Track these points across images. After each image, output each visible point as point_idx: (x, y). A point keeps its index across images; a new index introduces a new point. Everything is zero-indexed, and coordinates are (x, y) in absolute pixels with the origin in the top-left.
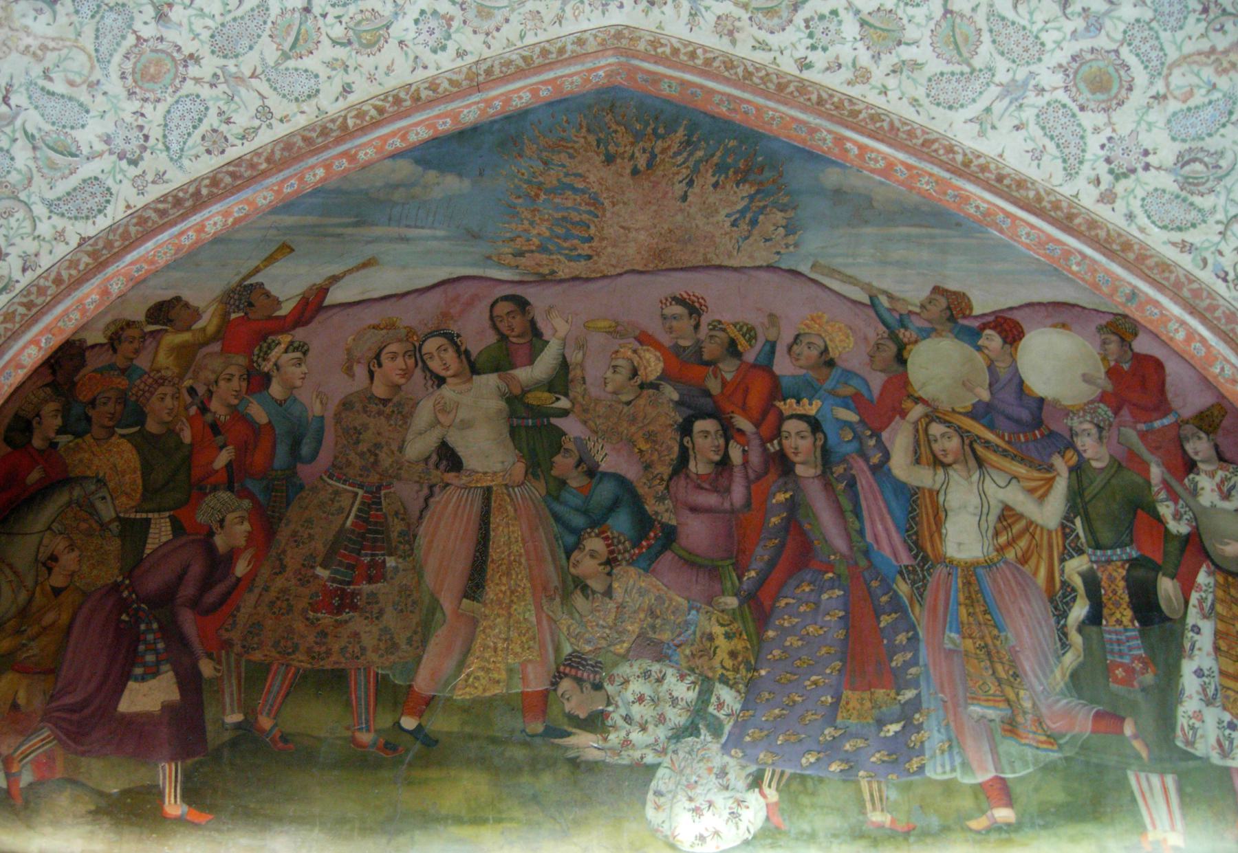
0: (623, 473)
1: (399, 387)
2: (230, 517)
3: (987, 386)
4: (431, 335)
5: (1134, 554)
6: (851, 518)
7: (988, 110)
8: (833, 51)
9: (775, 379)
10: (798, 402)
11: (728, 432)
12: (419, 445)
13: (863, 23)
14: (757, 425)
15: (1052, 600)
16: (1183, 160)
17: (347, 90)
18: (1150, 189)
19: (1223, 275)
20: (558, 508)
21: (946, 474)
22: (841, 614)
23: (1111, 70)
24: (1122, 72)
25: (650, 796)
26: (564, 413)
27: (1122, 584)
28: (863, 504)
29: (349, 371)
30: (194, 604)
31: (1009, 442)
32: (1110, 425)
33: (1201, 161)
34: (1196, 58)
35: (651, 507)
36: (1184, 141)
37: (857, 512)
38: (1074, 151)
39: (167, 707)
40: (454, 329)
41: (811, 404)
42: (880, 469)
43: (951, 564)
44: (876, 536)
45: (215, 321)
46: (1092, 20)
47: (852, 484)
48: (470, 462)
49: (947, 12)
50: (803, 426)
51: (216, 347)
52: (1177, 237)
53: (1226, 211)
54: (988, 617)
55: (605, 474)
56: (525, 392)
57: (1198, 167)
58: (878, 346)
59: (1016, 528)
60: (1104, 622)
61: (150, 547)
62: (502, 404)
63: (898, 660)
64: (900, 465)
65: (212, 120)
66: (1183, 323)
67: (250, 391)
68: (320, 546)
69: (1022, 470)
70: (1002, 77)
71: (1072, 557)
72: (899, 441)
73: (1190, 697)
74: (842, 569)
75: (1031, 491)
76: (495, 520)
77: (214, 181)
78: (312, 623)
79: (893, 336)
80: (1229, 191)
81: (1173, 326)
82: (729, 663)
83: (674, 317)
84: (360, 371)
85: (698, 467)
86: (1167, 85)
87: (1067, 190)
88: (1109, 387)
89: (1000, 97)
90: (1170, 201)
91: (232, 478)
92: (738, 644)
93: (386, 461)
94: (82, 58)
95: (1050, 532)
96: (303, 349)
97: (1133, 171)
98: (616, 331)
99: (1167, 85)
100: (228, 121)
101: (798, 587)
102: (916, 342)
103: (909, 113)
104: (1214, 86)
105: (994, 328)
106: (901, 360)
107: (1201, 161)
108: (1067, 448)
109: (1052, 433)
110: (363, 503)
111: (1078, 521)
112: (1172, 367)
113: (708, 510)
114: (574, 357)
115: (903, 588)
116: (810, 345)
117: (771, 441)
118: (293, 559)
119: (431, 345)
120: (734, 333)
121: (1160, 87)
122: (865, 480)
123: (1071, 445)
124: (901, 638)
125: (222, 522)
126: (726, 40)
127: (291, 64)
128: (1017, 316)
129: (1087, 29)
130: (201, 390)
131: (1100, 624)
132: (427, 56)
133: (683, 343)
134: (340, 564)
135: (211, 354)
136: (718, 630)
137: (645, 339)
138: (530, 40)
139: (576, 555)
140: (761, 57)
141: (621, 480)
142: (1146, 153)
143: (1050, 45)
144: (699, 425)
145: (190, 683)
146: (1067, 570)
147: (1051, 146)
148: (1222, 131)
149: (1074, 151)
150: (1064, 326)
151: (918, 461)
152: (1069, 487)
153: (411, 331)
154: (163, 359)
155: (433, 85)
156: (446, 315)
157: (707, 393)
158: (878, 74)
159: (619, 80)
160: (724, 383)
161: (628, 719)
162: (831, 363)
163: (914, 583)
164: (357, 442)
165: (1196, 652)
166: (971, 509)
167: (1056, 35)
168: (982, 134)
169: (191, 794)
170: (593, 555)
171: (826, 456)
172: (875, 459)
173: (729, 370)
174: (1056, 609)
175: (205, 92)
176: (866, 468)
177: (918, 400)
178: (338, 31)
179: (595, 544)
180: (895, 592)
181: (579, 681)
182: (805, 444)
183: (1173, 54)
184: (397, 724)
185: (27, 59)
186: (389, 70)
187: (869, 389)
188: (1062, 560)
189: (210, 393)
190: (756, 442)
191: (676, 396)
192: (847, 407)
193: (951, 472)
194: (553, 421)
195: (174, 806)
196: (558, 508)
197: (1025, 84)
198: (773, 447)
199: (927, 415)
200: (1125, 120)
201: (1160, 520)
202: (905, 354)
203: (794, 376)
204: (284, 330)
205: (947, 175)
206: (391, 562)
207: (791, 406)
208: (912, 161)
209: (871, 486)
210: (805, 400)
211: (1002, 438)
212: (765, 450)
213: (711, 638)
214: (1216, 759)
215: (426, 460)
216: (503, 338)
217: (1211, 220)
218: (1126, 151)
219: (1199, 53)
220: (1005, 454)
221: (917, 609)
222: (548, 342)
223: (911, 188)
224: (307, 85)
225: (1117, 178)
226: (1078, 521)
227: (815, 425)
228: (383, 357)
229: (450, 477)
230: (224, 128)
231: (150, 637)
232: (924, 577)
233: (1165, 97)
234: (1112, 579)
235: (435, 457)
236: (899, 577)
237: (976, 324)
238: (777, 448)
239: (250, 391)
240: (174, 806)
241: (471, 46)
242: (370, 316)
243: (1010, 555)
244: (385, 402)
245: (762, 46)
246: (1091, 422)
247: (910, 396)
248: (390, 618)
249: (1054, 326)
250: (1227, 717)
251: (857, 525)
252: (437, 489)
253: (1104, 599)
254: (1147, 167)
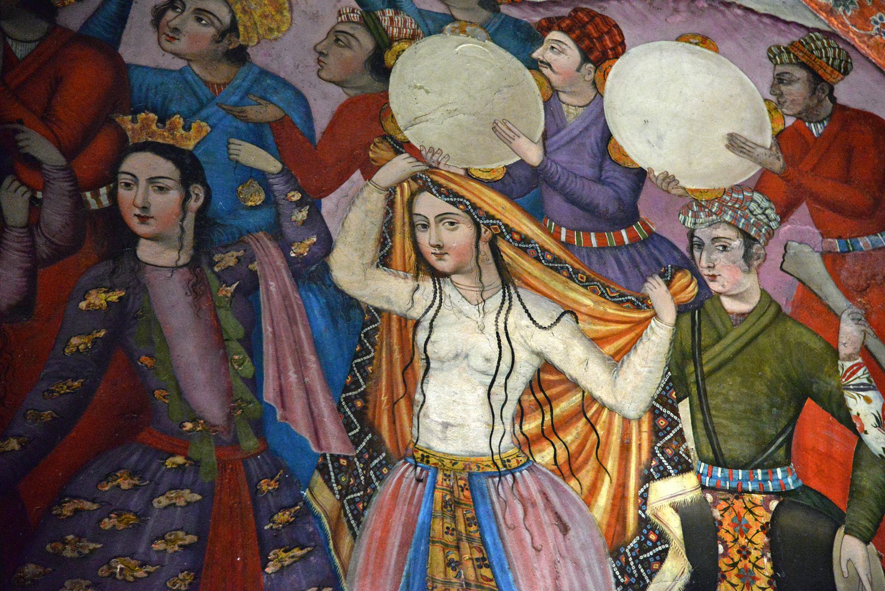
3: (538, 135)
5: (791, 483)
6: (238, 353)
9: (122, 69)
10: (162, 121)
14: (70, 152)
15: (615, 553)
21: (438, 291)
22: (190, 539)
27: (761, 539)
28: (267, 329)
31: (567, 245)
32: (771, 234)
41: (187, 128)
43: (424, 459)
50: (165, 167)
54: (486, 572)
58: (337, 37)
59: (563, 407)
69: (585, 300)
71: (664, 474)
72: (354, 216)
74: (207, 453)
75: (597, 341)
88: (778, 165)
95: (626, 420)
101: (106, 478)
102: (413, 38)
105: (567, 31)
106: (380, 69)
108: (678, 269)
109: (653, 238)
111: (684, 408)
115: (323, 498)
117: (94, 189)
122: (275, 285)
123: (689, 265)
151: (384, 261)
152: (673, 342)
163: (346, 490)
166: (477, 362)
171: (207, 232)
172: (300, 250)
174: (623, 570)
176: (280, 262)
177: (402, 146)
180: (306, 504)
192: (259, 142)
193: (448, 289)
199: (414, 178)
202: (389, 57)
207: (146, 125)
209: (285, 297)
210: (178, 120)
211: (556, 237)
212: (80, 203)
220: (555, 265)
221: (346, 540)
226: (684, 408)
227: (190, 169)
232: (368, 481)
234: (742, 528)
236: (317, 478)
238: (105, 202)
243: (544, 456)
247: (386, 137)
251: (248, 369)
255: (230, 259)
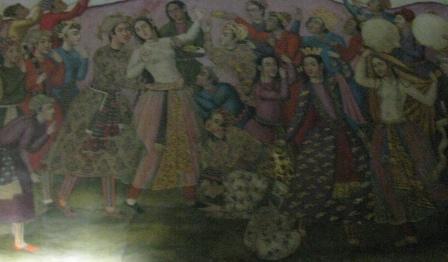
0: (228, 82)
1: (123, 44)
2: (45, 107)
4: (138, 20)
9: (300, 39)
11: (279, 63)
12: (133, 71)
20: (200, 100)
25: (246, 234)
26: (202, 55)
29: (100, 38)
30: (28, 148)
35: (243, 98)
39: (17, 197)
40: (148, 16)
42: (350, 80)
43: (385, 125)
44: (348, 110)
45: (37, 15)
47: (337, 86)
48: (158, 78)
50: (314, 60)
51: (36, 27)
55: (222, 84)
56: (183, 46)
58: (348, 22)
59: (414, 106)
61: (6, 121)
62: (172, 52)
63: (361, 168)
64: (359, 78)
67: (53, 47)
68: (87, 120)
69: (415, 79)
72: (359, 67)
75: (420, 89)
76: (171, 105)
78: (85, 156)
79: (355, 18)
82: (281, 171)
83: (253, 10)
84: (105, 37)
85: (265, 79)
91: (45, 89)
92: (286, 162)
93: (118, 78)
96: (78, 27)
98: (225, 17)
102: (365, 21)
106: (359, 29)
109: (429, 62)
110: (107, 99)
111: (442, 103)
113: (272, 100)
114: (206, 29)
115: (362, 134)
116: (316, 22)
118: (75, 125)
119: (138, 25)
120: (280, 16)
122: (344, 86)
123: (438, 68)
124: (362, 158)
125: (40, 109)
128: (412, 8)
130: (30, 46)
133: (258, 22)
134: (97, 127)
135: (35, 30)
136: (276, 156)
137: (239, 20)
139: (209, 122)
141: (227, 85)
144: (265, 60)
145: (27, 185)
150: (433, 13)
153: (129, 18)
154: (12, 33)
156: (146, 10)
157: (269, 45)
160: (276, 40)
161: (234, 198)
162: (326, 31)
164: (104, 71)
169: (28, 238)
170: (217, 121)
171: (325, 73)
172: (348, 75)
173: (278, 34)
177: (366, 47)
179: (217, 116)
181: (211, 181)
182: (315, 69)
184: (125, 203)
187: (343, 42)
189: (34, 48)
190: (291, 66)
191: (254, 47)
194: (197, 59)
195: (20, 243)
196: (200, 100)
198: (300, 69)
203: (310, 37)
204: (69, 19)
206: (121, 126)
213: (272, 159)
215: (137, 78)
216: (172, 20)
220: (408, 72)
222: (193, 23)
227: (319, 59)
228: (117, 29)
229: (148, 86)
231: (7, 164)
235: (141, 77)
237: (393, 12)
239: (53, 47)
240: (20, 243)
242: (110, 11)
244: (117, 51)
248: (121, 152)
249: (429, 13)
252: (142, 92)
255: (331, 80)
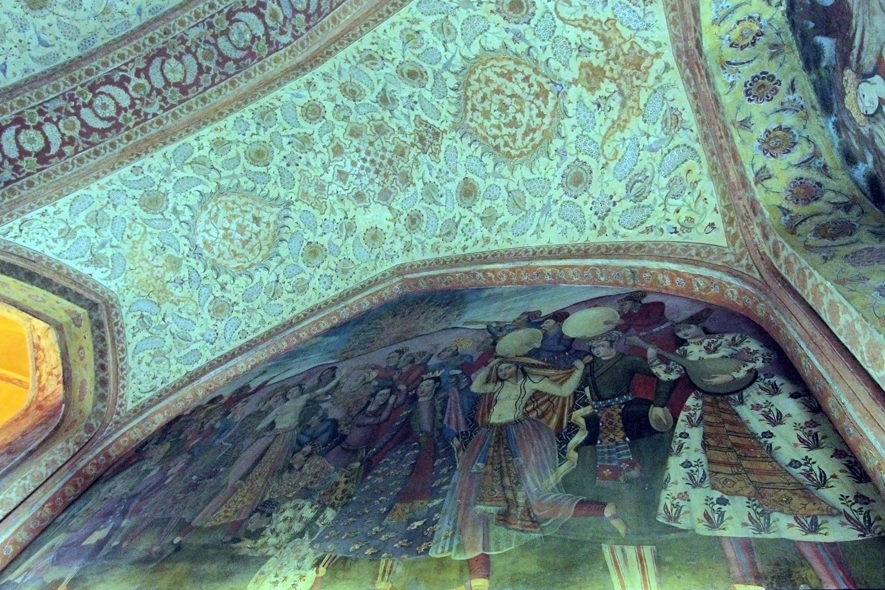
7: (538, 225)
8: (474, 237)
13: (482, 219)
16: (629, 188)
17: (293, 309)
18: (620, 213)
19: (674, 230)
23: (579, 170)
24: (584, 167)
33: (637, 181)
34: (609, 133)
36: (625, 177)
37: (443, 412)
38: (579, 219)
46: (561, 153)
47: (445, 400)
49: (509, 192)
52: (643, 228)
53: (661, 196)
57: (638, 185)
60: (599, 442)
65: (243, 326)
66: (662, 271)
70: (539, 207)
73: (676, 483)
77: (240, 348)
80: (657, 185)
81: (660, 277)
86: (605, 157)
87: (582, 240)
89: (541, 216)
90: (632, 213)
94: (194, 305)
97: (609, 210)
99: (605, 157)
100: (249, 326)
103: (507, 246)
104: (624, 139)
107: (637, 181)
112: (669, 303)
121: (603, 161)
126: (436, 253)
127: (272, 302)
129: (562, 159)
131: (596, 443)
132: (323, 292)
138: (364, 278)
140: (449, 253)
142: (611, 197)
143: (551, 178)
146: (573, 417)
147: (569, 224)
148: (640, 158)
149: (579, 219)
150: (596, 306)
155: (326, 303)
158: (493, 237)
159: (407, 290)
165: (683, 450)
167: (551, 172)
168: (539, 237)
175: (240, 316)
178: (289, 288)
183: (599, 140)
185: (172, 305)
186: (310, 300)
188: (571, 411)
197: (549, 202)
200: (595, 189)
201: (655, 376)
205: (526, 263)
208: (511, 266)
214: (703, 530)
217: (656, 208)
218: (602, 203)
219: (609, 129)
223: (522, 283)
224: (277, 310)
225: (603, 219)
230: (247, 329)
233: (607, 163)
241: (342, 285)
245: (449, 249)
246: (606, 340)
250: (717, 494)
253: (601, 429)
254: (615, 204)
